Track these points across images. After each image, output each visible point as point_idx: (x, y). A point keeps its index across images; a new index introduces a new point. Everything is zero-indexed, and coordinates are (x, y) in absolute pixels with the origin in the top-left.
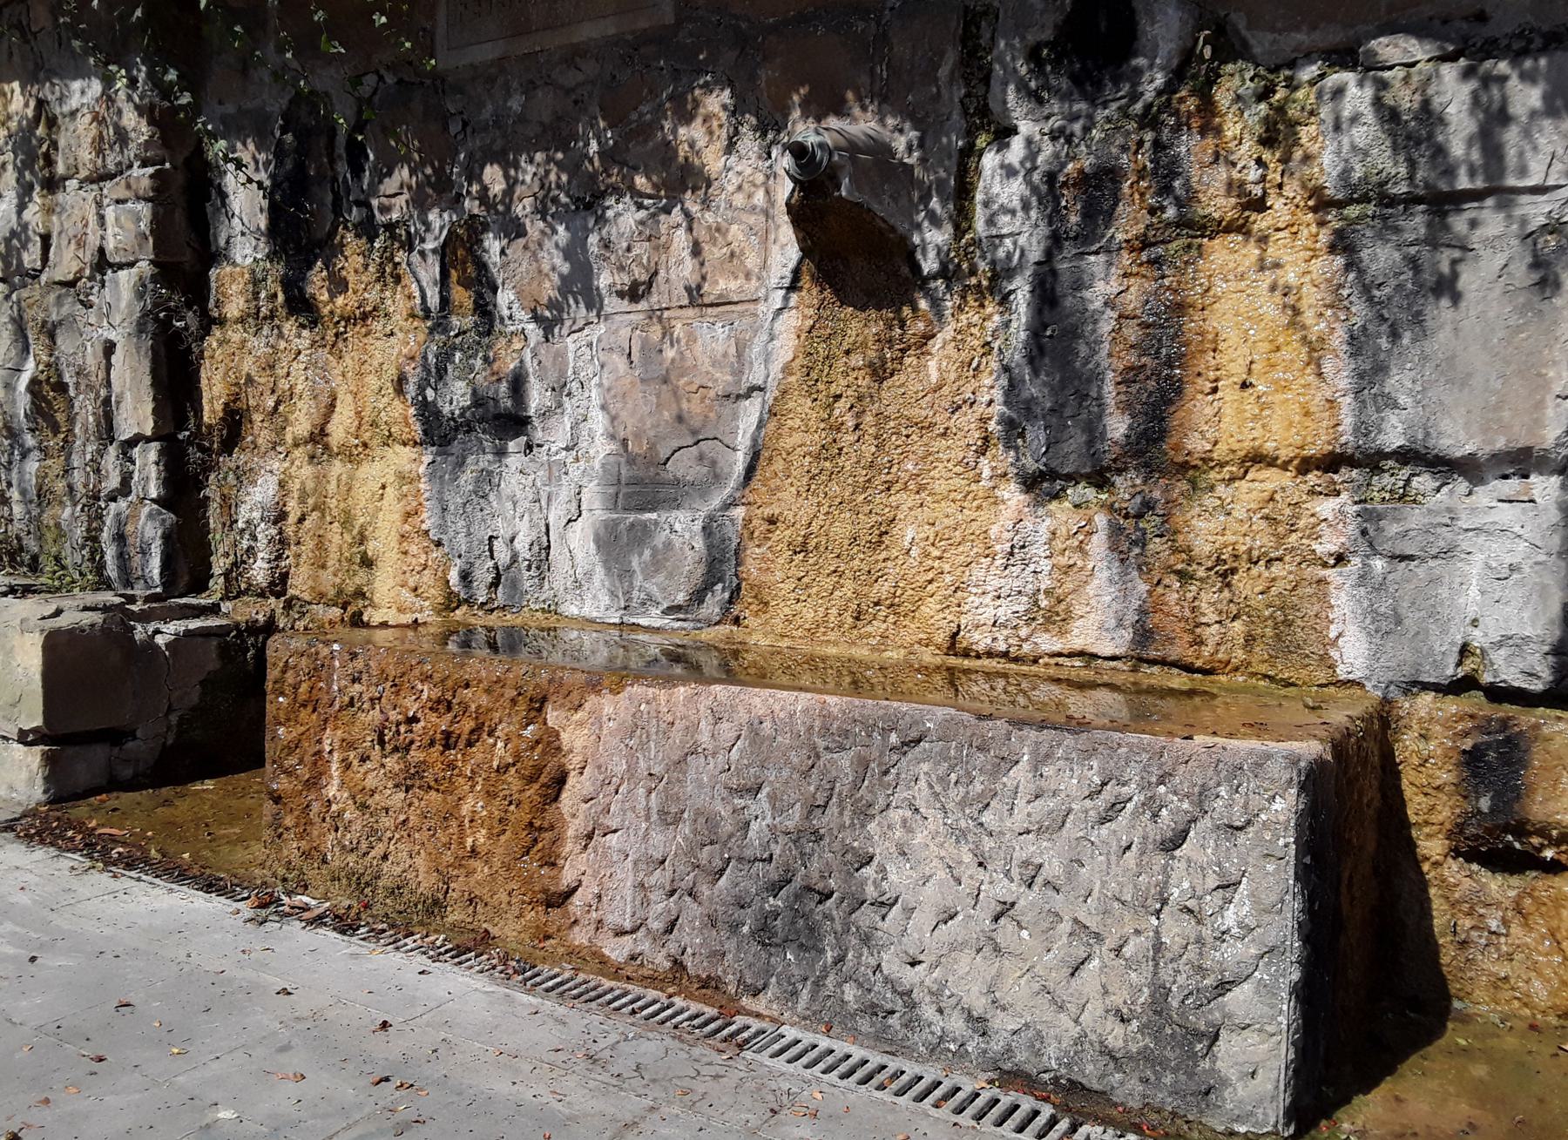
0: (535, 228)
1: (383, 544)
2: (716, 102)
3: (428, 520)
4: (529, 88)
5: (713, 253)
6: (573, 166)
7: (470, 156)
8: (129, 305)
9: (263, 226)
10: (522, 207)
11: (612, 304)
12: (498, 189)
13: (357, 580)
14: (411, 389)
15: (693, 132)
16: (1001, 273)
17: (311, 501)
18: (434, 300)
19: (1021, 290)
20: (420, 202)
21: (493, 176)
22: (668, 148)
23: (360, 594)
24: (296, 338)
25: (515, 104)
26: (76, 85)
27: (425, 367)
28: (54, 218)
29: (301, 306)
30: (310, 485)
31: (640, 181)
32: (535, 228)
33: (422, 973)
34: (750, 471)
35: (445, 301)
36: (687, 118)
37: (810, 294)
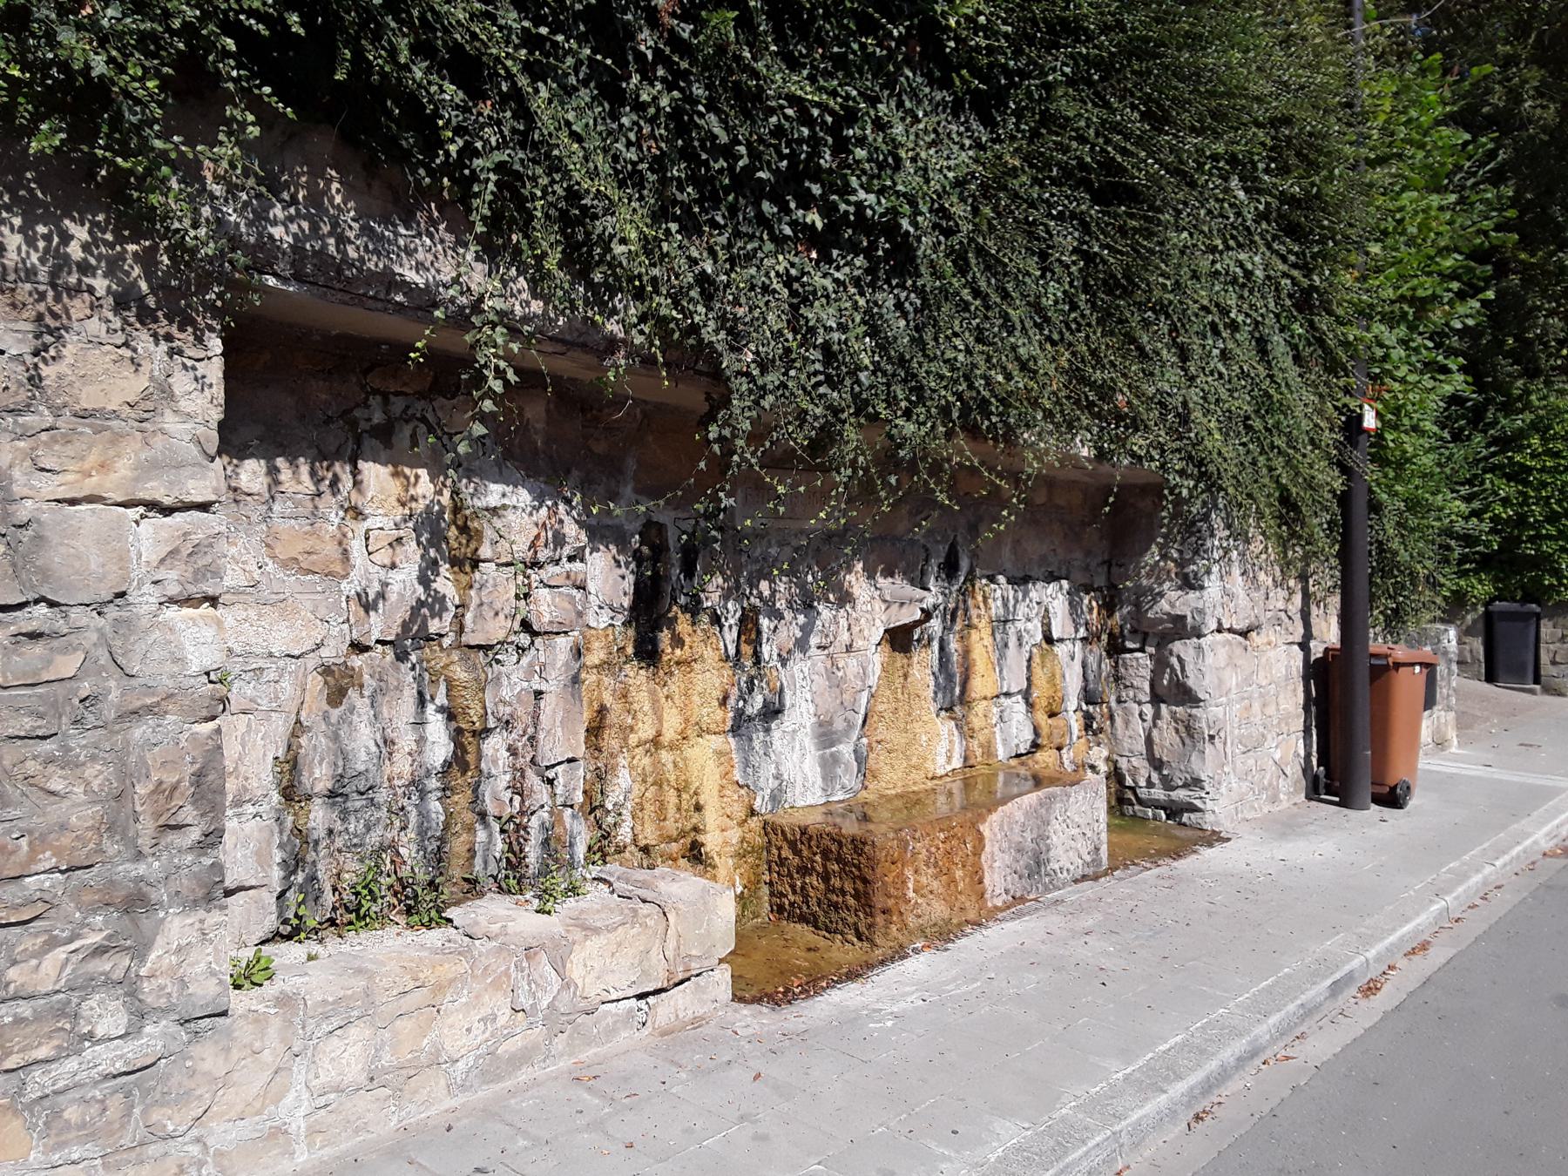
0: (788, 615)
1: (709, 798)
2: (859, 566)
3: (737, 775)
4: (781, 545)
5: (855, 629)
6: (802, 586)
7: (750, 574)
8: (566, 664)
9: (626, 605)
10: (781, 604)
11: (813, 651)
12: (767, 593)
13: (694, 821)
14: (732, 702)
15: (850, 578)
16: (930, 640)
17: (650, 780)
18: (732, 651)
19: (936, 645)
20: (726, 597)
21: (764, 586)
22: (841, 584)
23: (696, 829)
24: (636, 676)
25: (773, 551)
26: (493, 487)
27: (740, 690)
28: (473, 593)
29: (647, 653)
30: (649, 769)
31: (831, 596)
32: (788, 615)
33: (478, 1170)
34: (864, 722)
35: (738, 651)
36: (850, 572)
37: (886, 648)
